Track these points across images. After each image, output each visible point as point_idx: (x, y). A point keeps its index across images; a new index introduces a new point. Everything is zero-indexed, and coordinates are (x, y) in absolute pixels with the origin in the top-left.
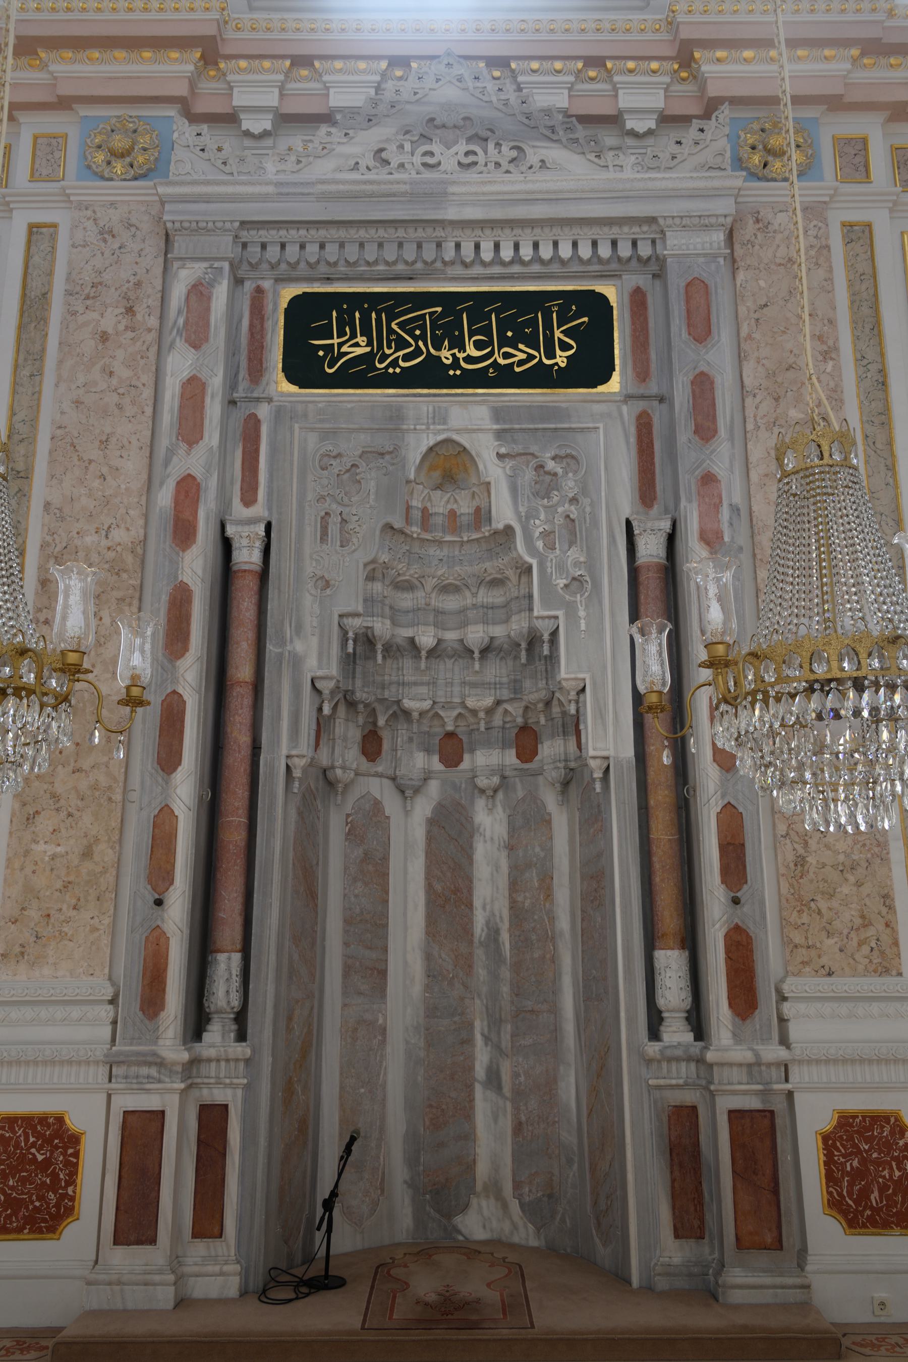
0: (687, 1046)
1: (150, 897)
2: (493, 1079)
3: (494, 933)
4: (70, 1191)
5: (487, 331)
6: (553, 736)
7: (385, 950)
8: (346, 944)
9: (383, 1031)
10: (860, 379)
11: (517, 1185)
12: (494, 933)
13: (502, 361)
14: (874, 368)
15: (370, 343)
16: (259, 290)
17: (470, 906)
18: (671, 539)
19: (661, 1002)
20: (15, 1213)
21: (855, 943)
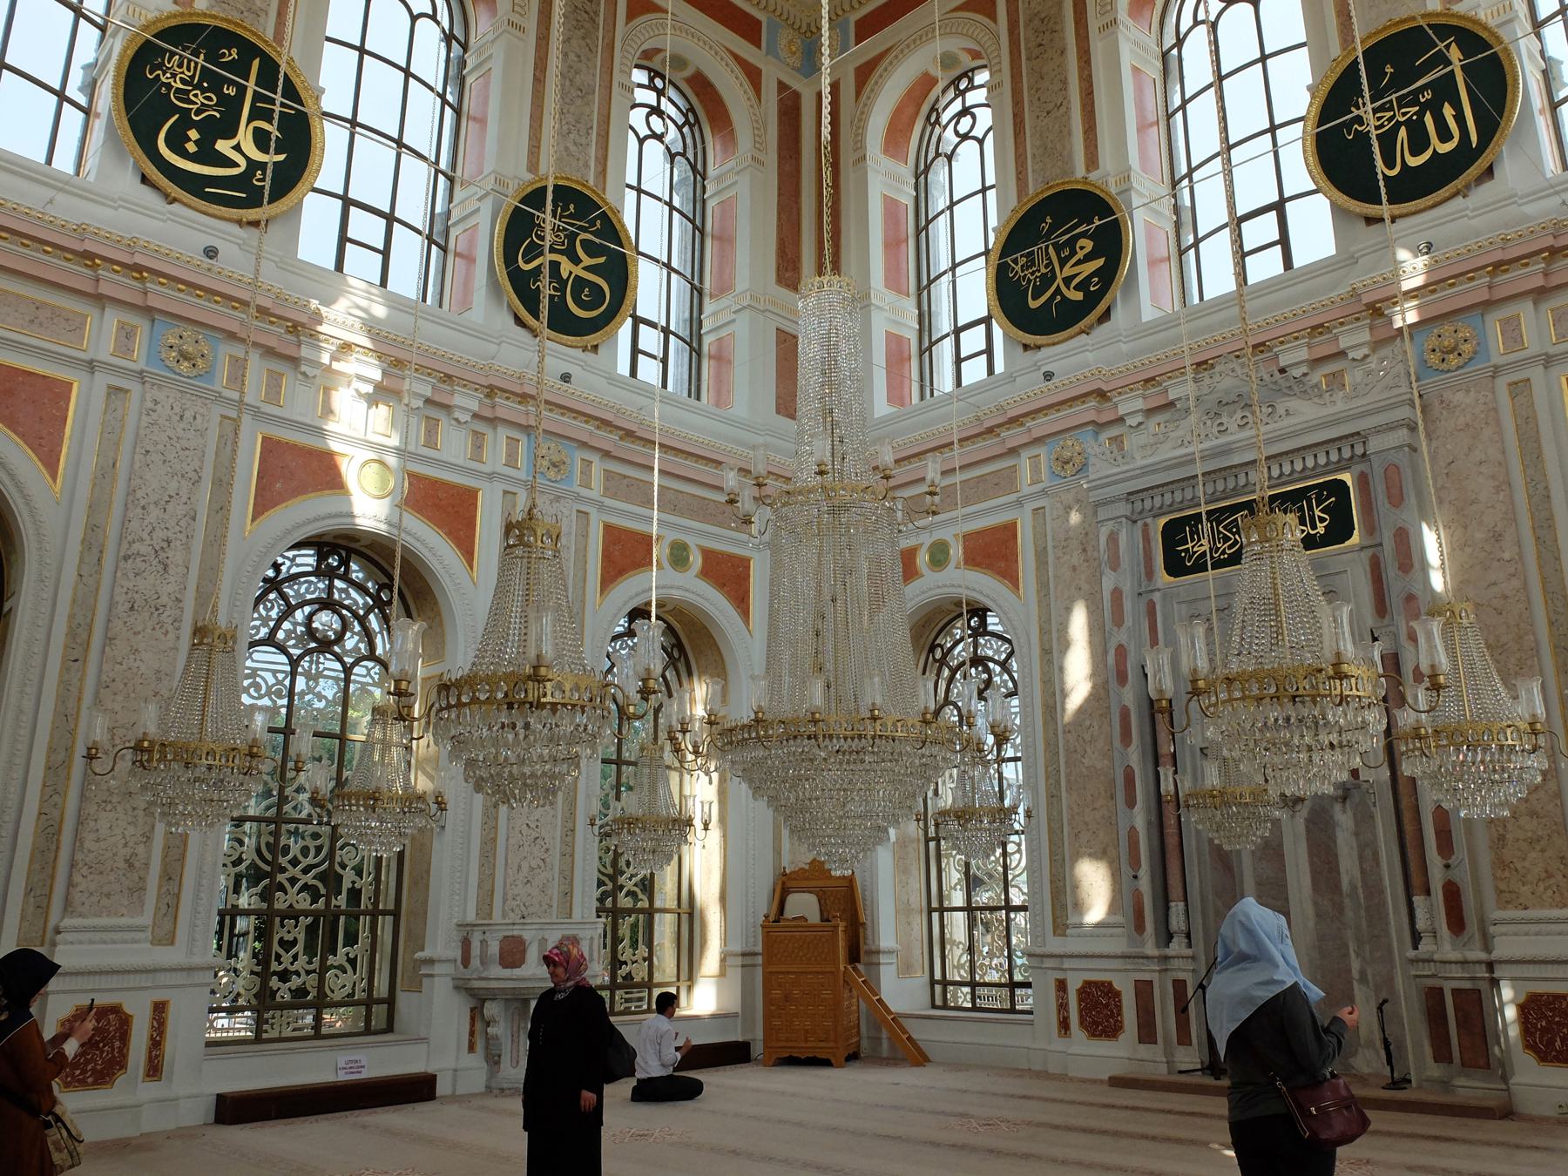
2: (1363, 979)
3: (1354, 888)
10: (1530, 497)
16: (1146, 525)
17: (1338, 873)
21: (1542, 888)
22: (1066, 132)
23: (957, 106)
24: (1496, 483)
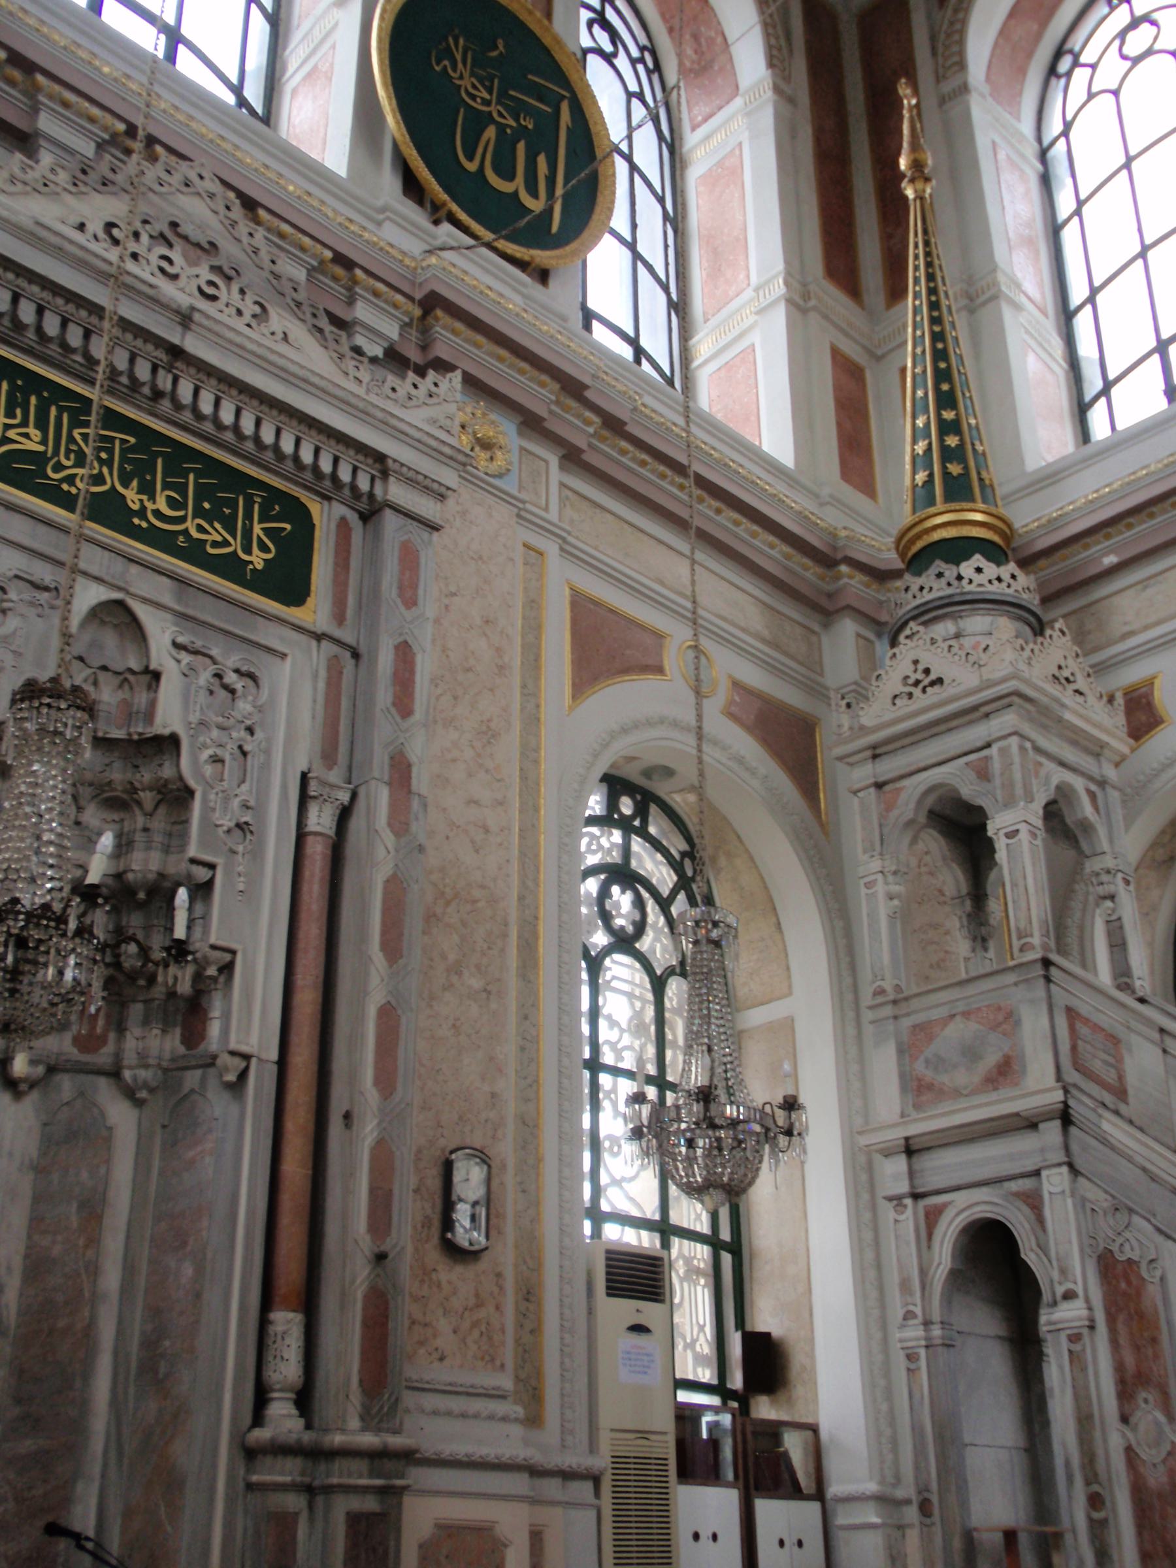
5: (182, 489)
6: (146, 1022)
13: (195, 534)
15: (44, 442)
18: (345, 814)
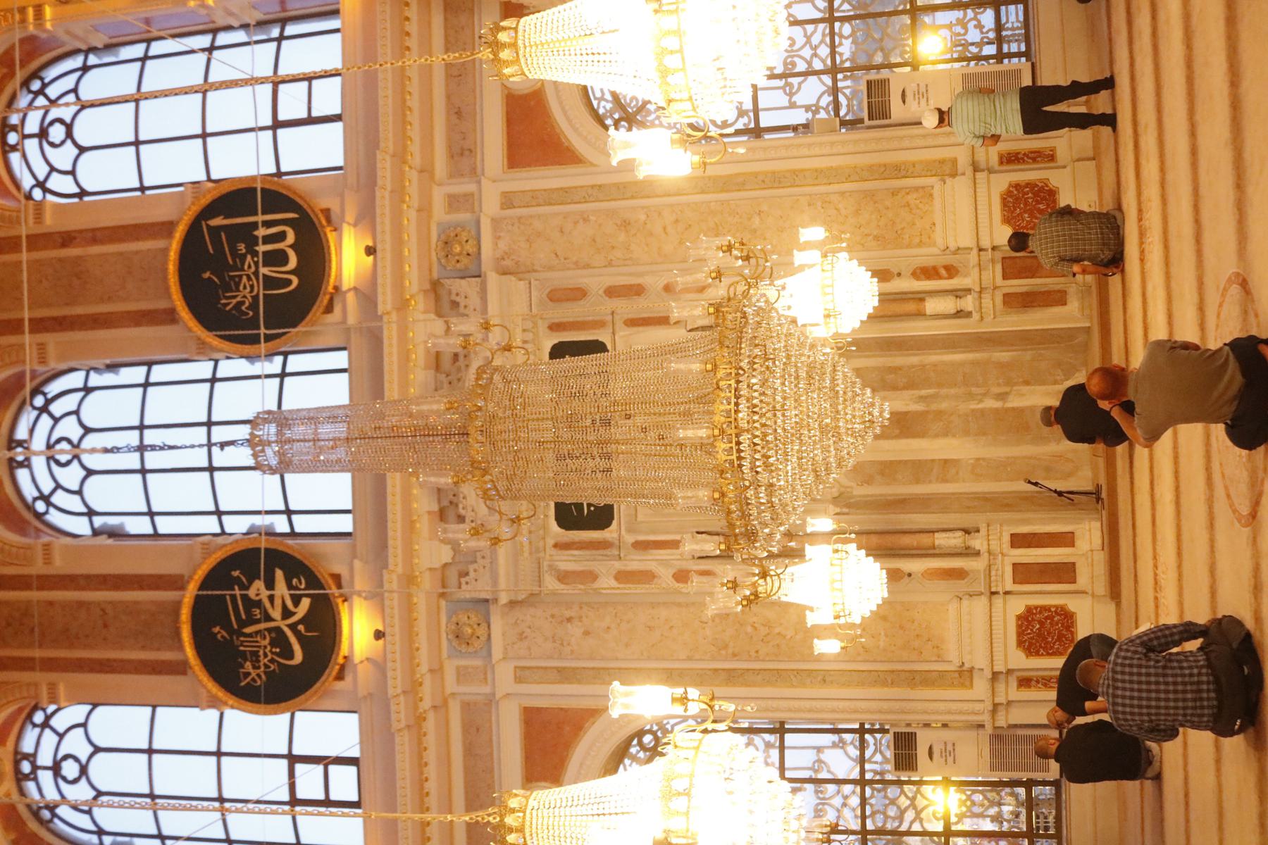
0: (974, 298)
1: (906, 579)
2: (1002, 397)
3: (922, 399)
4: (1053, 609)
7: (933, 461)
8: (930, 482)
9: (978, 459)
11: (1056, 382)
12: (922, 399)
14: (590, 191)
17: (906, 413)
19: (953, 311)
20: (1064, 636)
22: (132, 609)
23: (46, 777)
24: (581, 221)
